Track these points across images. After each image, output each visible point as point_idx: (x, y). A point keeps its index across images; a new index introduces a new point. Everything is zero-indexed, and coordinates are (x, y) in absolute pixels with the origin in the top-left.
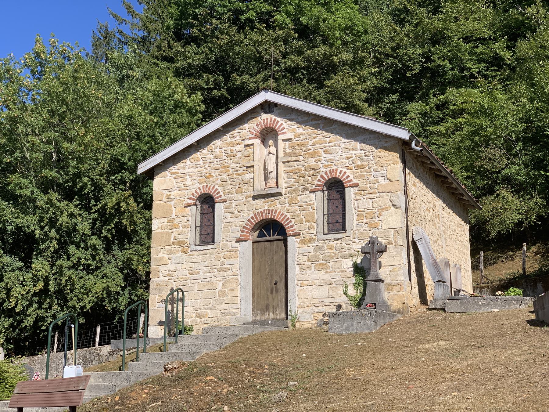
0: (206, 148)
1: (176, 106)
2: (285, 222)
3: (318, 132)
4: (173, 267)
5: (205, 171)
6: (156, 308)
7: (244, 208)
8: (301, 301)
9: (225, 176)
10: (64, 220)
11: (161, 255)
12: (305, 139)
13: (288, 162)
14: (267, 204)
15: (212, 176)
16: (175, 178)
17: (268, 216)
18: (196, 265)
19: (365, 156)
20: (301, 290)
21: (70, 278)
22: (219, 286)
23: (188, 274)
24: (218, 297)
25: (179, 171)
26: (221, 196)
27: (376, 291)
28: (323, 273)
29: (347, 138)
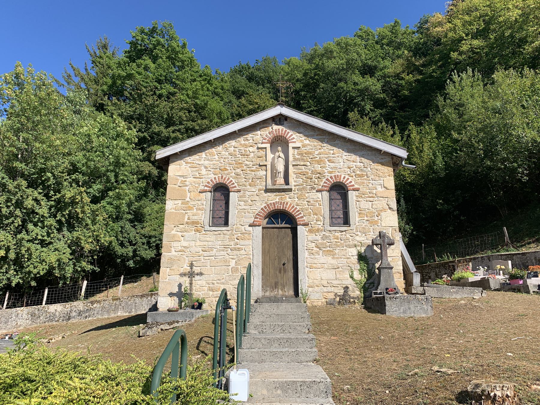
0: (221, 146)
1: (118, 136)
2: (295, 213)
3: (323, 145)
4: (185, 244)
5: (220, 165)
6: (167, 280)
7: (257, 198)
8: (311, 281)
9: (238, 171)
10: (29, 203)
11: (173, 232)
12: (311, 149)
13: (297, 165)
14: (278, 197)
15: (227, 170)
16: (190, 167)
17: (280, 207)
18: (210, 243)
19: (364, 167)
20: (310, 272)
21: (29, 249)
22: (233, 263)
23: (201, 251)
24: (231, 274)
25: (194, 162)
26: (235, 187)
27: (389, 277)
28: (330, 258)
29: (348, 152)
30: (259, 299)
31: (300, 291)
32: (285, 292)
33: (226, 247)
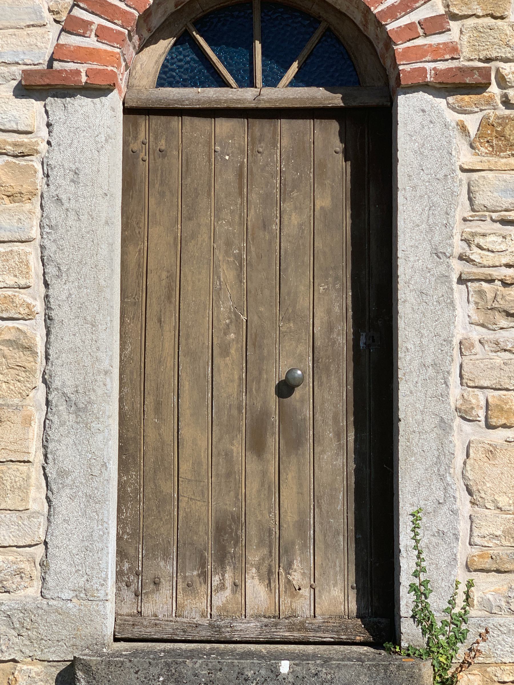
20: (491, 452)
30: (87, 668)
31: (406, 602)
32: (294, 591)
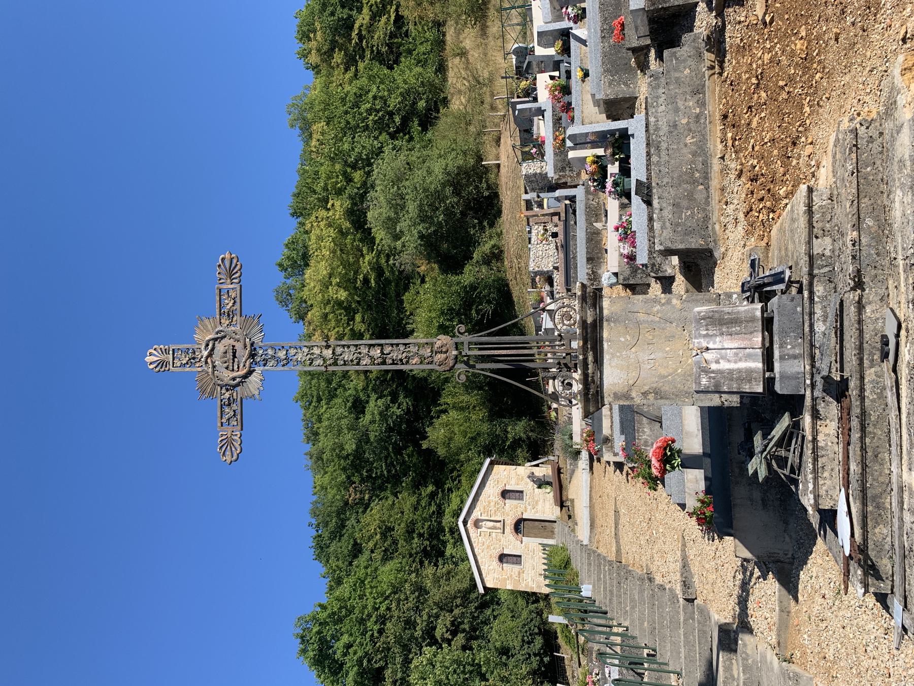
1: (431, 664)
33: (533, 557)
